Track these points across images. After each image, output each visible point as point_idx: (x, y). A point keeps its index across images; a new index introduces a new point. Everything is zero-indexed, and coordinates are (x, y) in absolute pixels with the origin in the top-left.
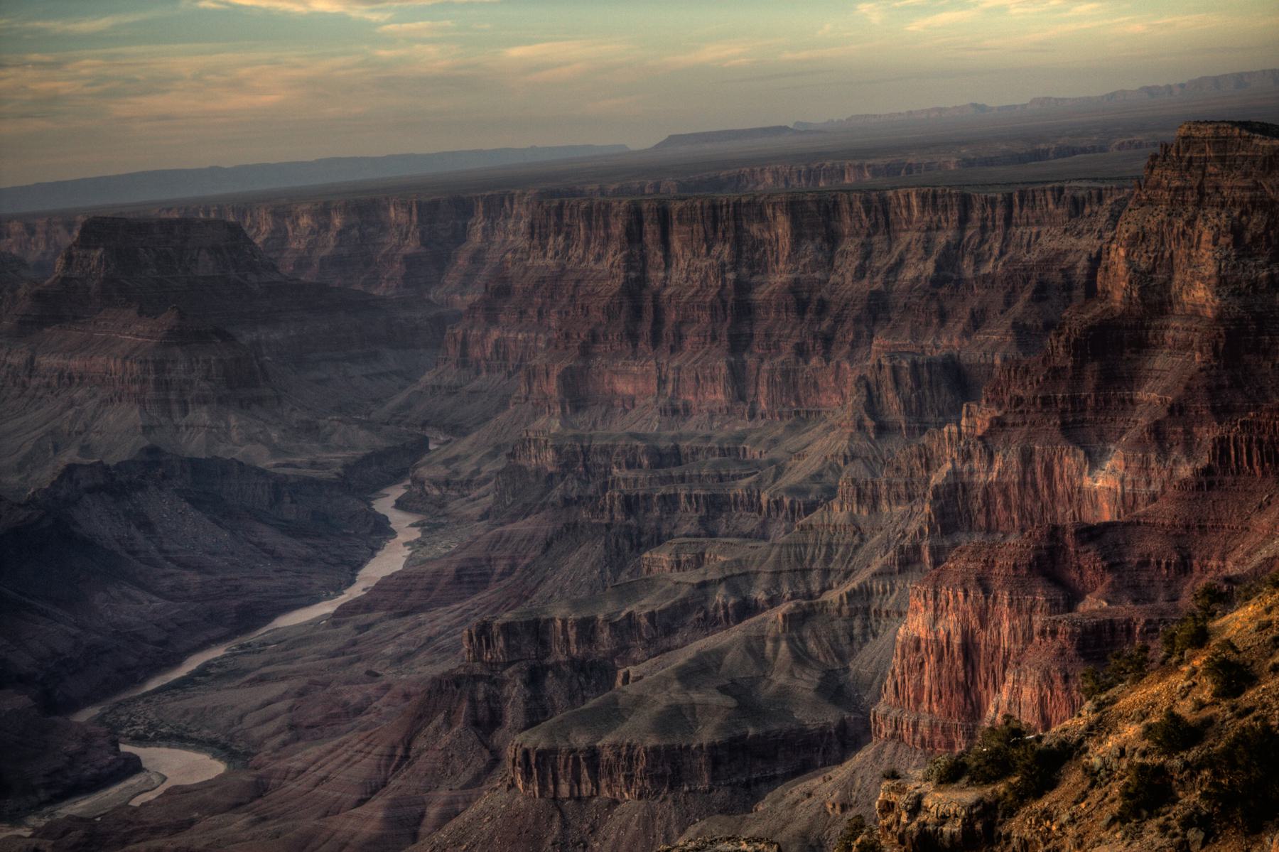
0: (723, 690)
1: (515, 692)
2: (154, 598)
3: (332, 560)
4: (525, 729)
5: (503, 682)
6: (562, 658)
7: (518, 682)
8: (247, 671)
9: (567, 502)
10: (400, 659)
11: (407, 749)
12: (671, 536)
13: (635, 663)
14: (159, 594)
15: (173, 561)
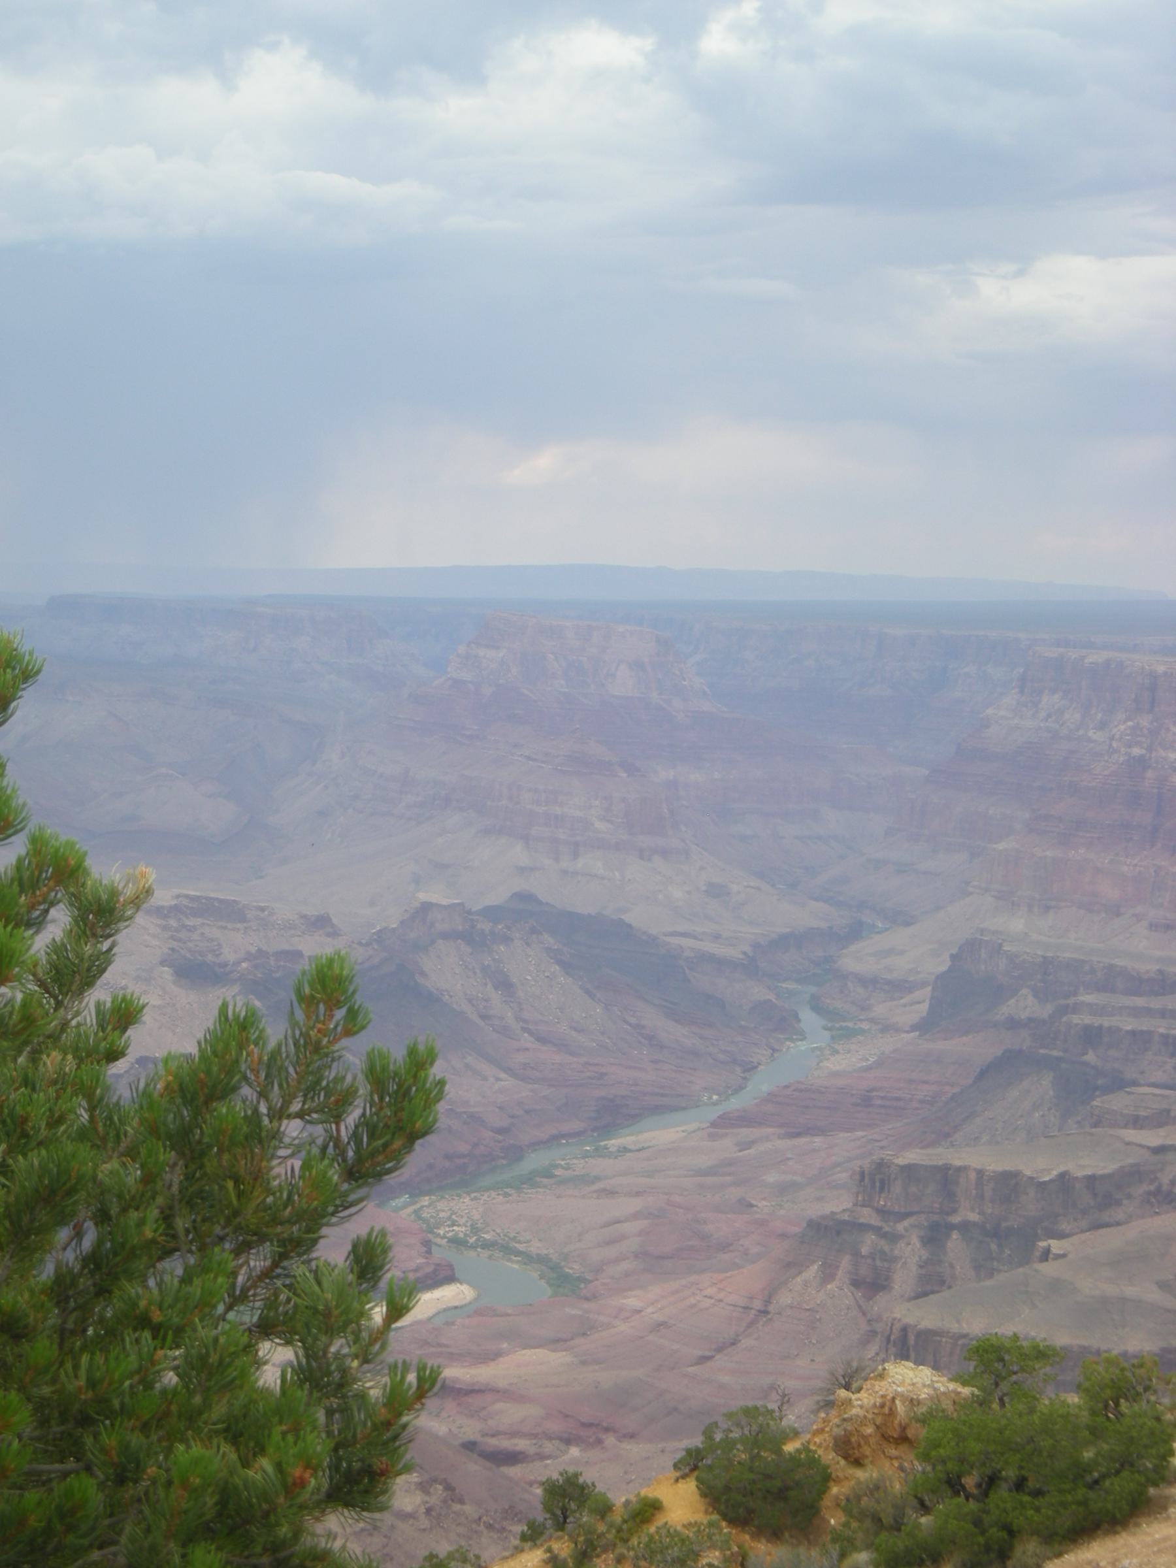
0: (1163, 1286)
1: (911, 1251)
2: (503, 1075)
3: (722, 1057)
4: (910, 1299)
5: (893, 1238)
6: (974, 1217)
7: (915, 1241)
8: (597, 1179)
9: (1013, 1024)
10: (783, 1189)
11: (768, 1302)
12: (1135, 1083)
13: (1061, 1236)
14: (509, 1071)
15: (531, 1033)
